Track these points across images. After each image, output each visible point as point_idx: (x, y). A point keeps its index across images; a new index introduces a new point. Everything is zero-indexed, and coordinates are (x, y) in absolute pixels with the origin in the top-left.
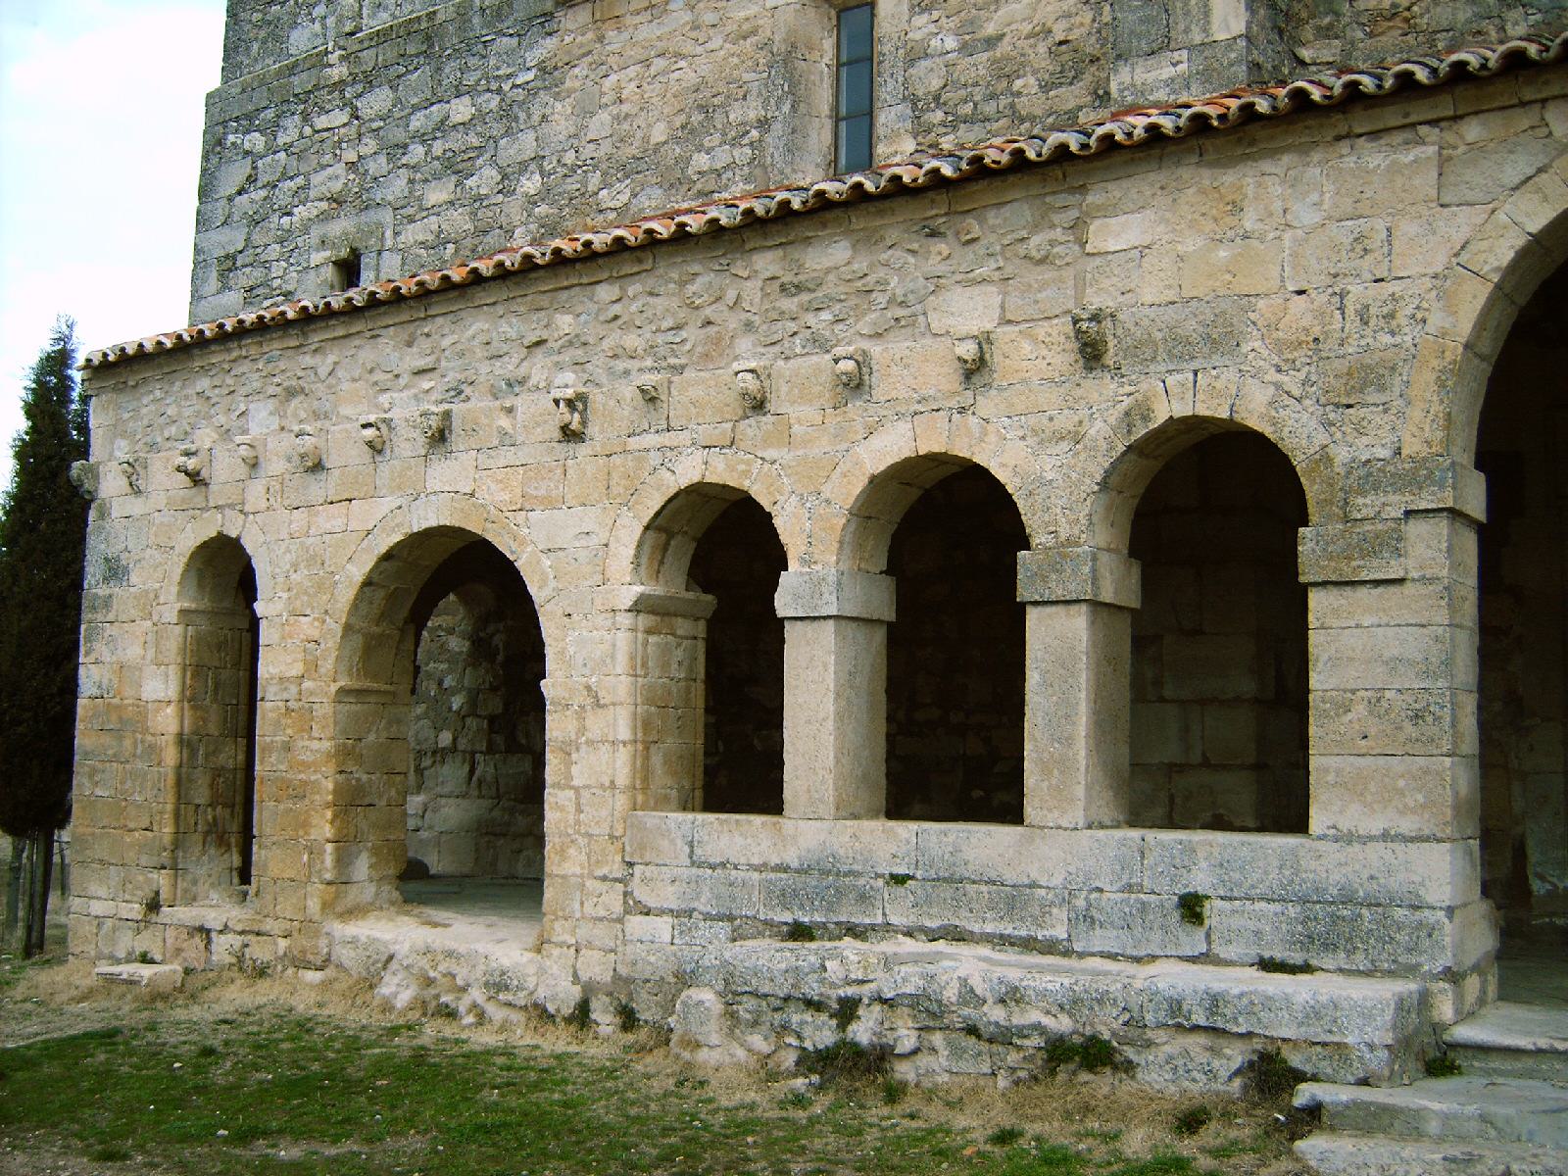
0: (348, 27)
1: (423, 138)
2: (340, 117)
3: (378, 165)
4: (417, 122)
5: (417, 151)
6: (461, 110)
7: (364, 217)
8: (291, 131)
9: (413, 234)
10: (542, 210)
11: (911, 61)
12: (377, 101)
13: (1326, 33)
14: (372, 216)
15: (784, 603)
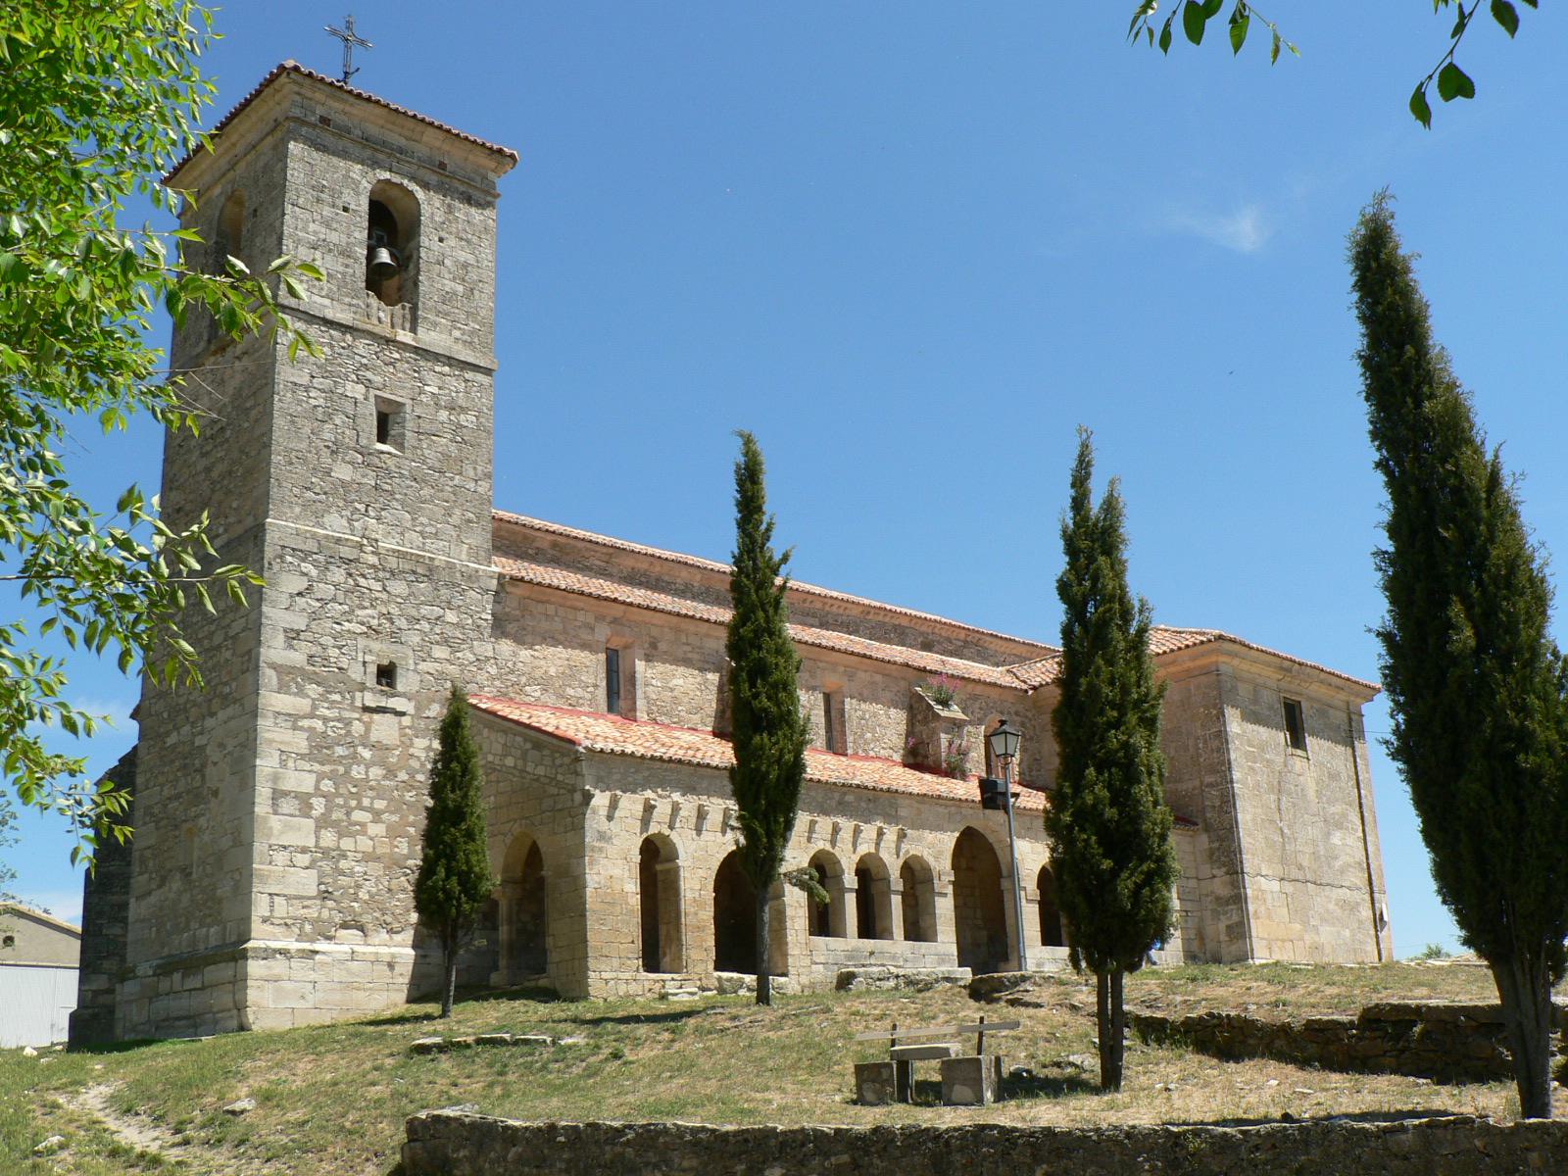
3: (402, 623)
4: (425, 610)
6: (451, 617)
7: (394, 647)
9: (423, 666)
11: (646, 685)
12: (398, 587)
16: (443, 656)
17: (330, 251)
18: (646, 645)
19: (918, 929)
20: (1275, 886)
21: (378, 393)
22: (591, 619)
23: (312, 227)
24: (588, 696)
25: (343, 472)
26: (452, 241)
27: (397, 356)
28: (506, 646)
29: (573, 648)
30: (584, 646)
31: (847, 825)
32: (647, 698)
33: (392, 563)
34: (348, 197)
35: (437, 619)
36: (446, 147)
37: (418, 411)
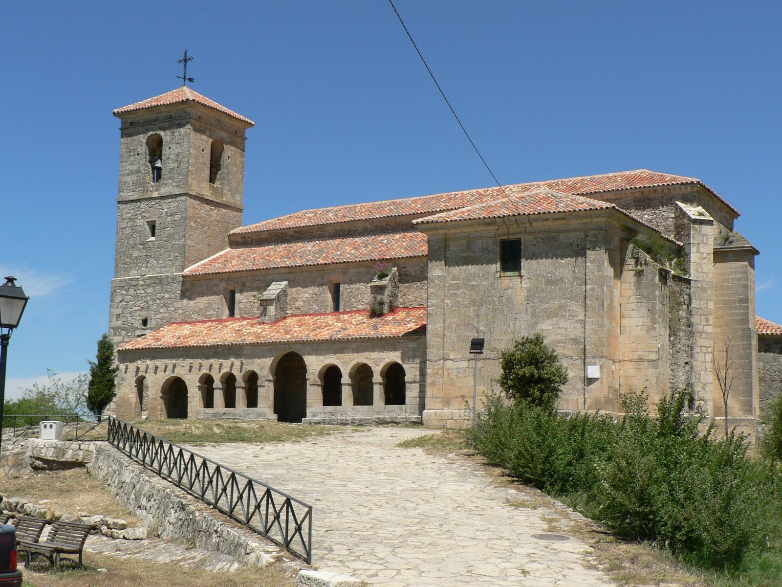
0: (144, 274)
1: (159, 299)
2: (142, 292)
3: (151, 303)
5: (158, 301)
6: (167, 296)
8: (132, 291)
9: (157, 316)
10: (182, 316)
11: (240, 303)
12: (150, 290)
13: (291, 309)
14: (149, 312)
15: (214, 386)
16: (164, 311)
17: (133, 173)
18: (240, 286)
19: (252, 401)
20: (464, 364)
21: (147, 220)
22: (218, 282)
23: (128, 167)
24: (215, 313)
25: (136, 254)
26: (173, 146)
27: (154, 203)
28: (185, 301)
29: (210, 295)
30: (215, 293)
31: (237, 363)
32: (240, 309)
33: (148, 281)
34: (139, 150)
35: (163, 297)
36: (169, 109)
37: (160, 221)
